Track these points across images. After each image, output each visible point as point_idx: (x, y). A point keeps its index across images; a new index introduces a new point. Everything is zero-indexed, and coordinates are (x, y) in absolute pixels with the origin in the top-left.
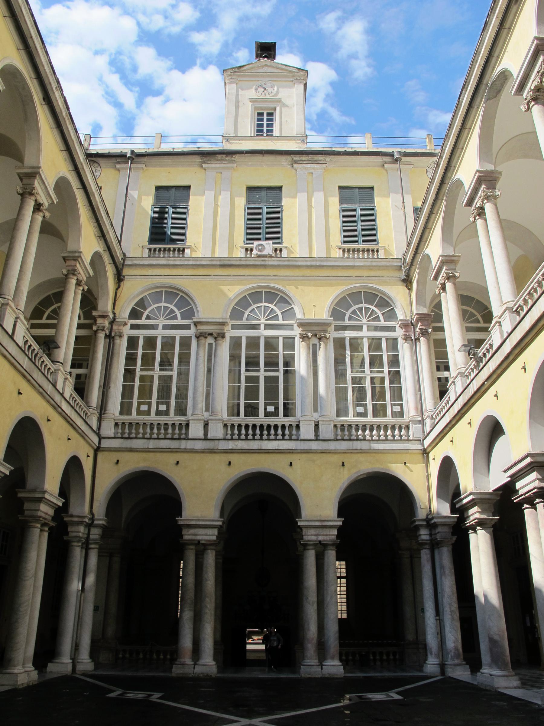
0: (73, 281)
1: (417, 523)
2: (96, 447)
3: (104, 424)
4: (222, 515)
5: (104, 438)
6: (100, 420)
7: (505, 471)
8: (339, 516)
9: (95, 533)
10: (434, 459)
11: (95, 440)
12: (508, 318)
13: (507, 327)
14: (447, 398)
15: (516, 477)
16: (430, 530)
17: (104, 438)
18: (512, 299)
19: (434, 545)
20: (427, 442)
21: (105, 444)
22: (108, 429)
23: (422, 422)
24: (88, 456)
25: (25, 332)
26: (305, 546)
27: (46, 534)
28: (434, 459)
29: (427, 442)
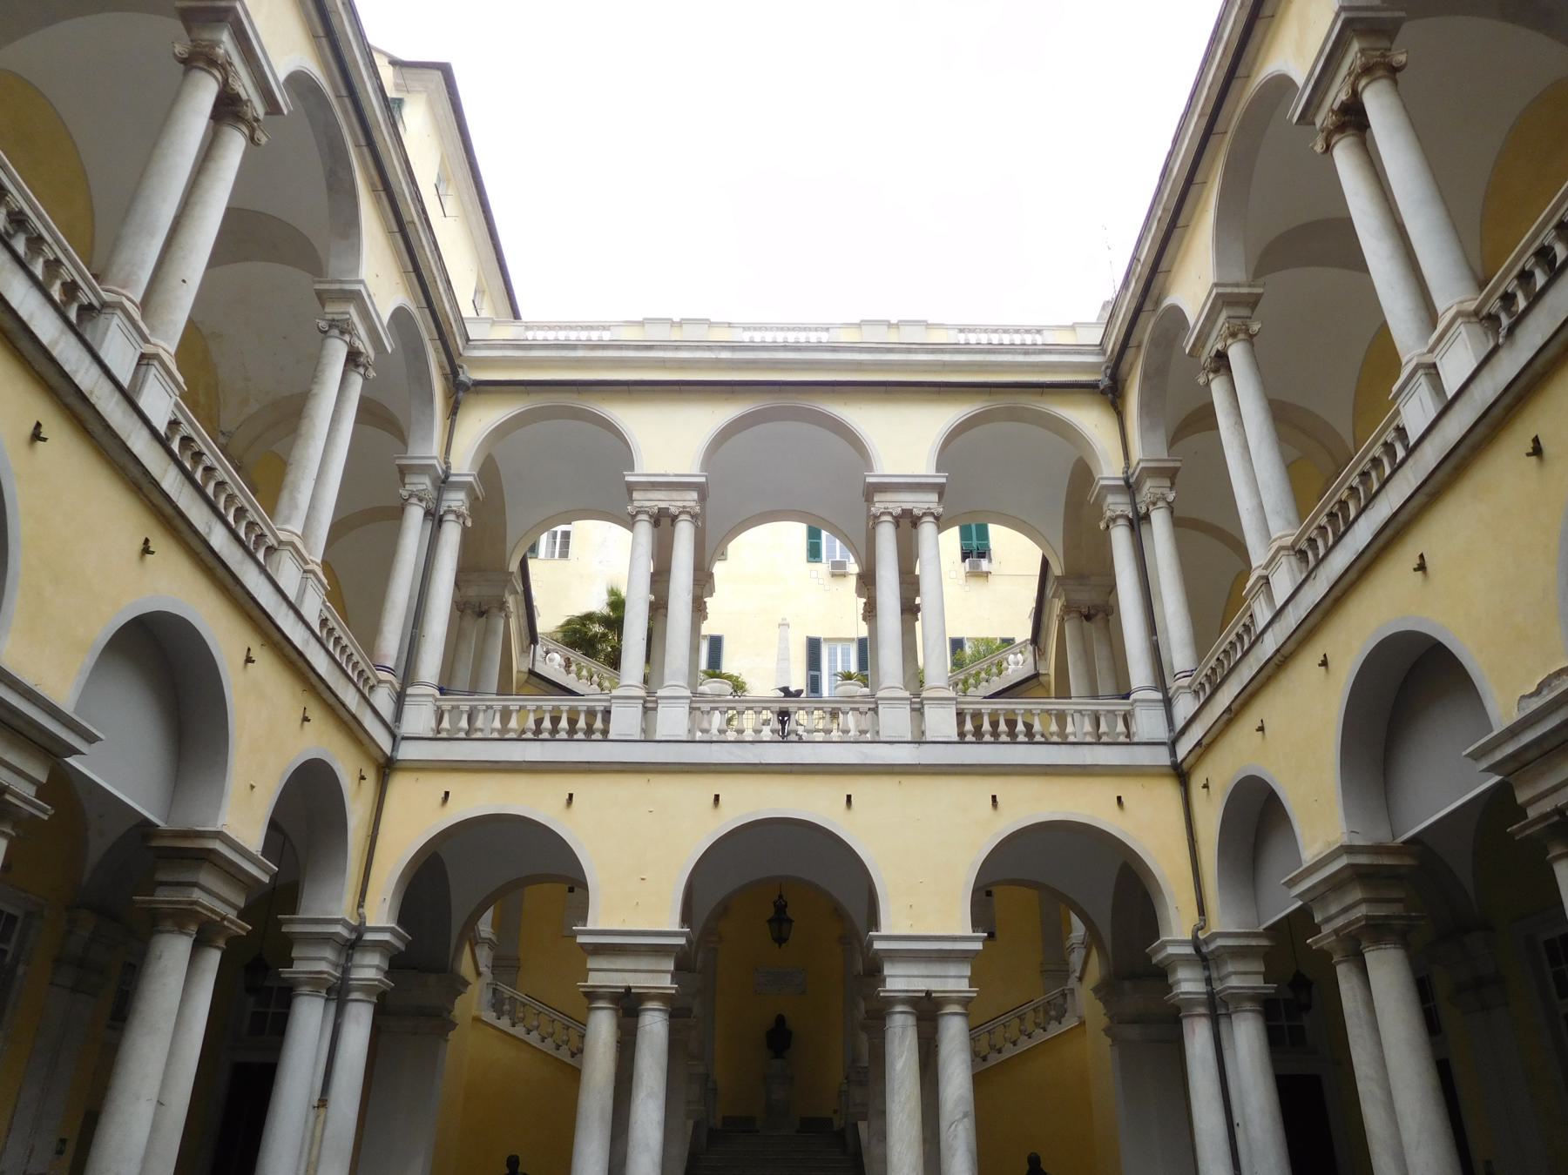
0: (337, 352)
1: (1171, 950)
2: (382, 760)
3: (410, 712)
4: (687, 916)
5: (404, 738)
6: (400, 699)
7: (1477, 756)
8: (976, 923)
9: (369, 969)
10: (1206, 786)
11: (385, 742)
12: (1464, 334)
13: (1282, 584)
14: (1239, 629)
15: (1520, 766)
16: (1206, 968)
17: (404, 738)
18: (1469, 296)
19: (1218, 1009)
20: (1183, 749)
21: (407, 752)
22: (418, 719)
23: (1168, 703)
24: (363, 778)
25: (177, 405)
26: (891, 1002)
27: (213, 959)
28: (1206, 786)
29: (1183, 749)
